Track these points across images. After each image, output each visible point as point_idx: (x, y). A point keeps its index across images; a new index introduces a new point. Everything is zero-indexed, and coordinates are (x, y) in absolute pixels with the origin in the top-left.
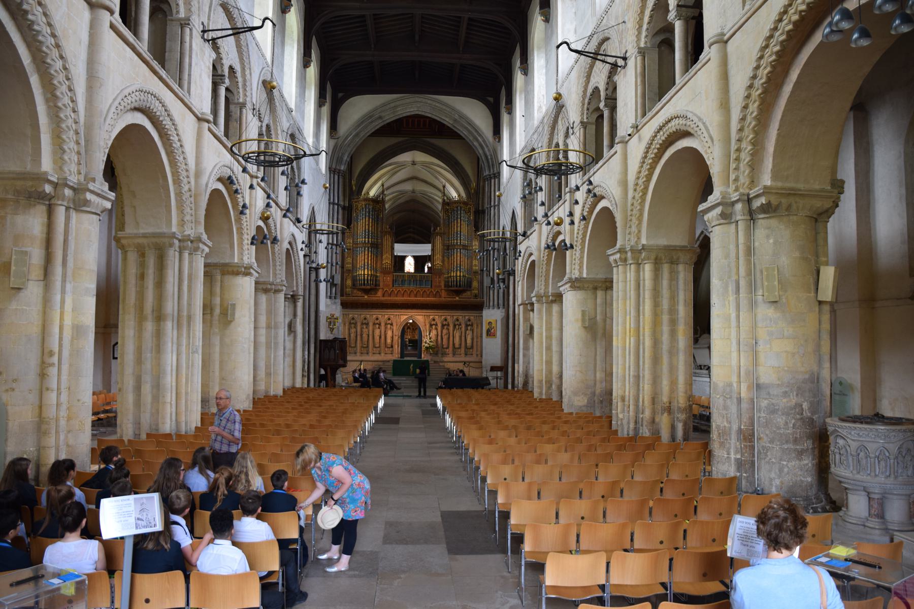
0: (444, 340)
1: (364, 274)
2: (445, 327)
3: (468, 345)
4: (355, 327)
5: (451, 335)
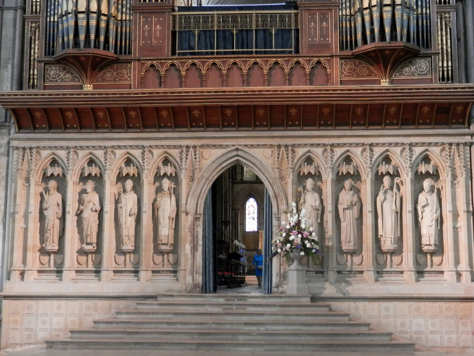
0: (343, 225)
1: (76, 13)
2: (348, 183)
3: (425, 241)
4: (62, 189)
5: (368, 208)
